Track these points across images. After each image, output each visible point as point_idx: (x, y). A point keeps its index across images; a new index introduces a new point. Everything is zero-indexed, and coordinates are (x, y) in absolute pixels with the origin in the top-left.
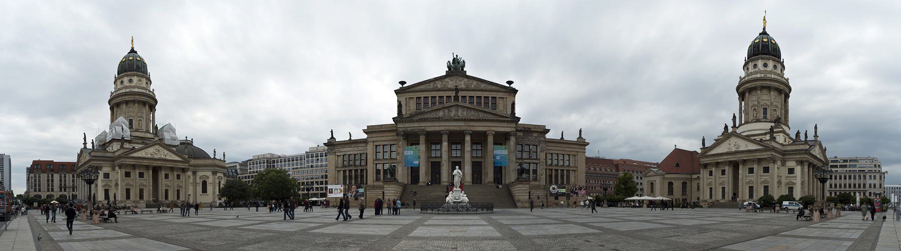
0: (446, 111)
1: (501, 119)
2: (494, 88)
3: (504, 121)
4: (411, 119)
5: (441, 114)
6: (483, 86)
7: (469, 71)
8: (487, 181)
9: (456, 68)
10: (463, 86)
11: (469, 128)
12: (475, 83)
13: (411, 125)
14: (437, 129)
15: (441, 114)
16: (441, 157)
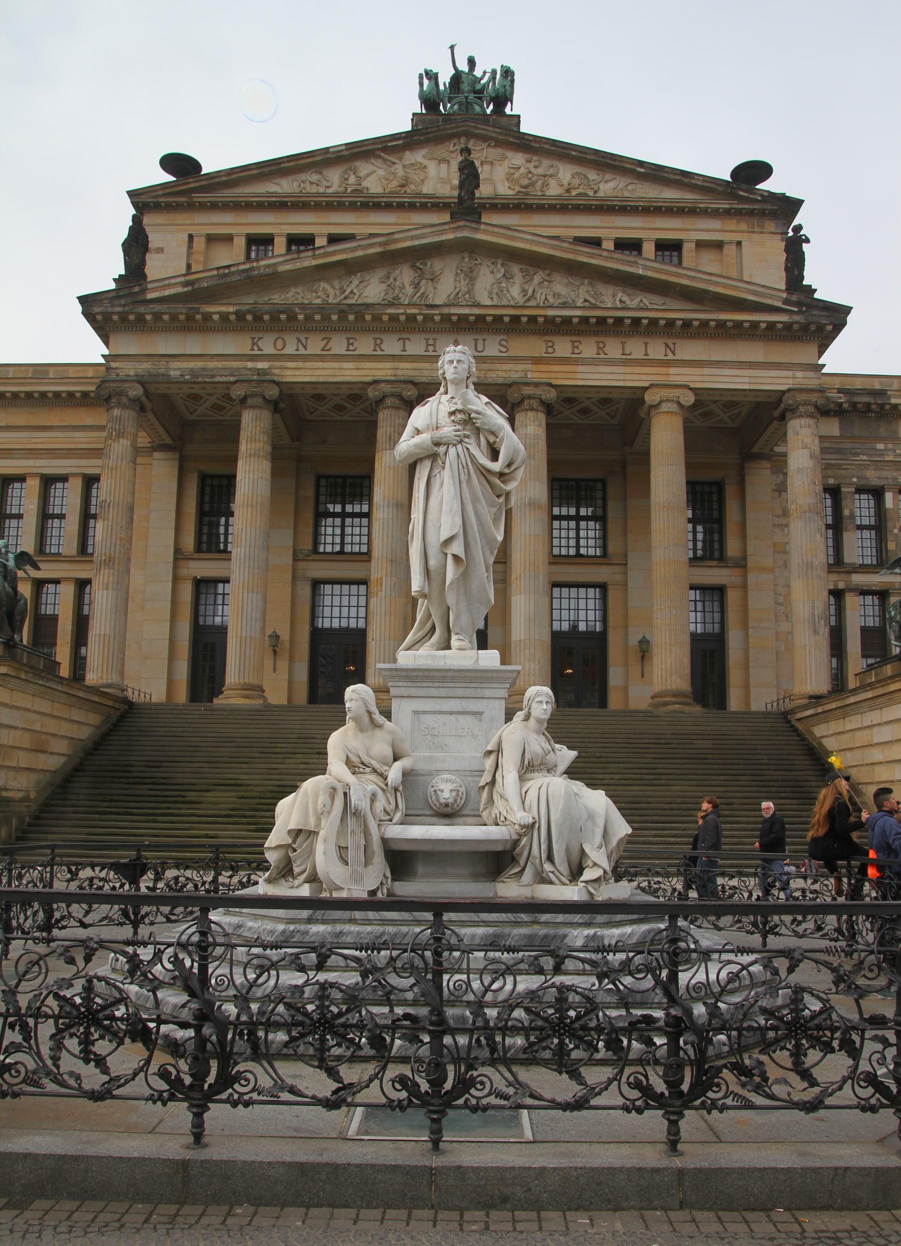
0: (405, 275)
1: (724, 317)
2: (670, 194)
3: (750, 332)
4: (191, 309)
5: (371, 290)
6: (609, 187)
7: (534, 114)
8: (640, 697)
9: (466, 111)
10: (504, 190)
11: (535, 374)
12: (566, 173)
13: (193, 344)
14: (348, 373)
15: (371, 290)
16: (366, 557)
